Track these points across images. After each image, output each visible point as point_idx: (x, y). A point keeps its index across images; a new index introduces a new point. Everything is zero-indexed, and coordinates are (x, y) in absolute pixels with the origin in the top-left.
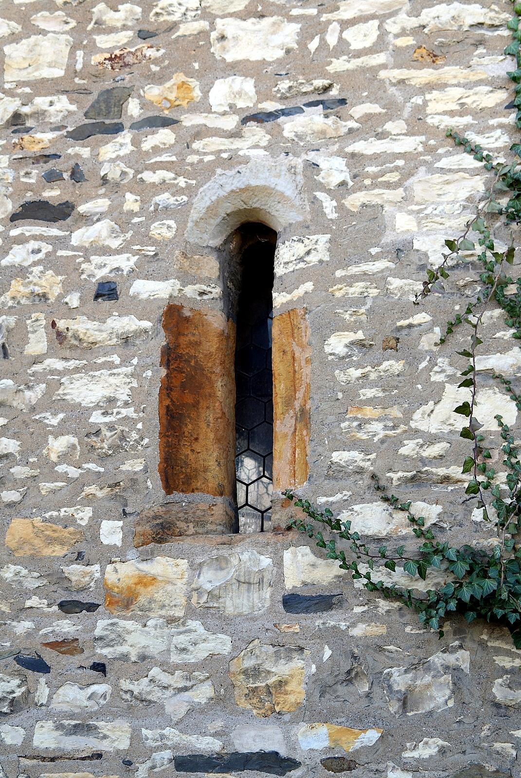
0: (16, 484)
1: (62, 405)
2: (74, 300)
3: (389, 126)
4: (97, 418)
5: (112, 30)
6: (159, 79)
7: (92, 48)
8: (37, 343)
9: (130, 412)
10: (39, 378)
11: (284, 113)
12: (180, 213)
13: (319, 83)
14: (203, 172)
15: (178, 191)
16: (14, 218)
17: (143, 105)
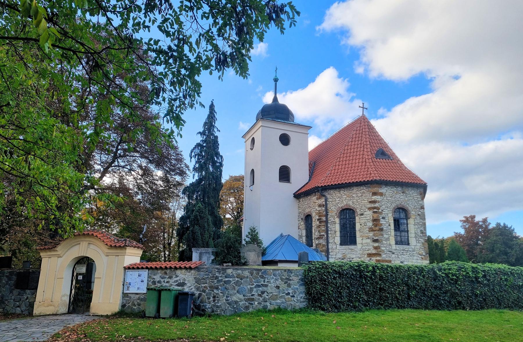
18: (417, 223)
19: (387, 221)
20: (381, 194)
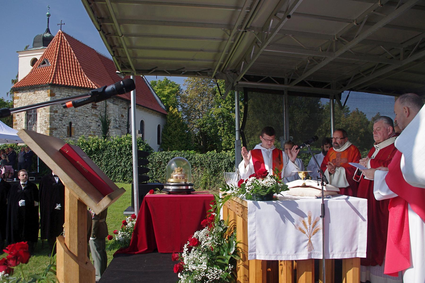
8: (61, 127)
12: (68, 122)
18: (43, 115)
19: (20, 117)
20: (18, 98)
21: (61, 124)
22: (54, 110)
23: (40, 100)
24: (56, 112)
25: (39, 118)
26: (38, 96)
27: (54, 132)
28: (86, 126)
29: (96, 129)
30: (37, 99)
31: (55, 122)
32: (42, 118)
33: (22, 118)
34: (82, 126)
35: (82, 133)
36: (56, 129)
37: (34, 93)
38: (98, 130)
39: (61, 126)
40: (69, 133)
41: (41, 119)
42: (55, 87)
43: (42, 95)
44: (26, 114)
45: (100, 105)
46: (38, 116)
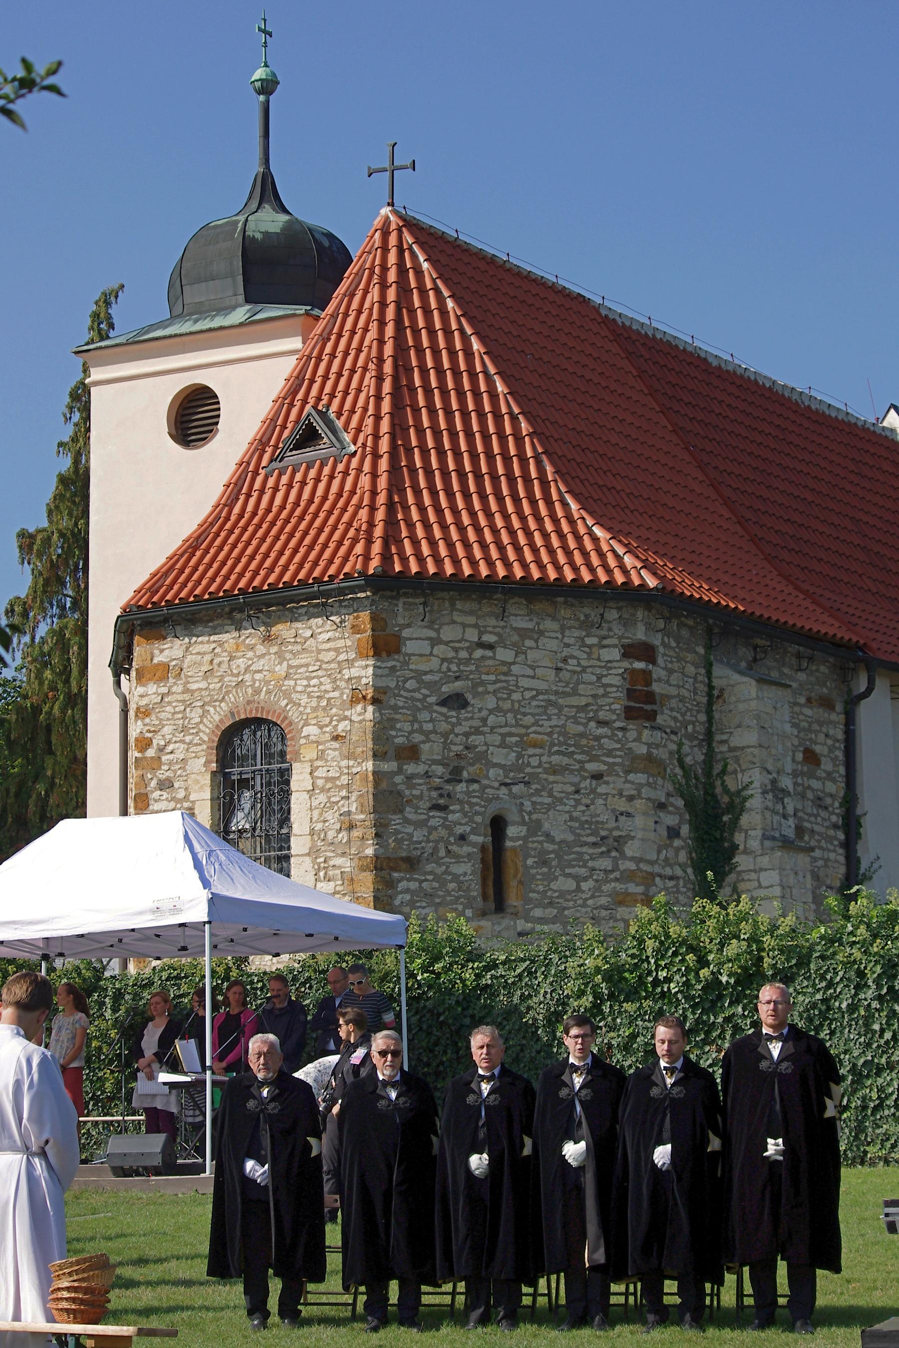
0: (439, 897)
1: (450, 873)
2: (452, 839)
3: (543, 793)
4: (461, 878)
5: (456, 744)
6: (472, 765)
7: (450, 750)
8: (442, 853)
9: (471, 877)
10: (444, 864)
11: (513, 784)
13: (522, 775)
14: (489, 801)
15: (483, 807)
16: (430, 809)
17: (469, 774)
18: (327, 779)
19: (181, 794)
20: (162, 673)
21: (443, 833)
22: (397, 740)
23: (309, 679)
24: (411, 753)
25: (306, 796)
26: (295, 654)
27: (402, 885)
28: (592, 839)
29: (659, 852)
30: (287, 677)
31: (407, 821)
32: (322, 798)
33: (192, 798)
34: (570, 838)
35: (571, 884)
36: (411, 863)
37: (268, 639)
38: (666, 859)
39: (441, 846)
40: (491, 891)
41: (315, 803)
42: (396, 598)
43: (319, 651)
44: (213, 773)
45: (673, 691)
46: (294, 785)
